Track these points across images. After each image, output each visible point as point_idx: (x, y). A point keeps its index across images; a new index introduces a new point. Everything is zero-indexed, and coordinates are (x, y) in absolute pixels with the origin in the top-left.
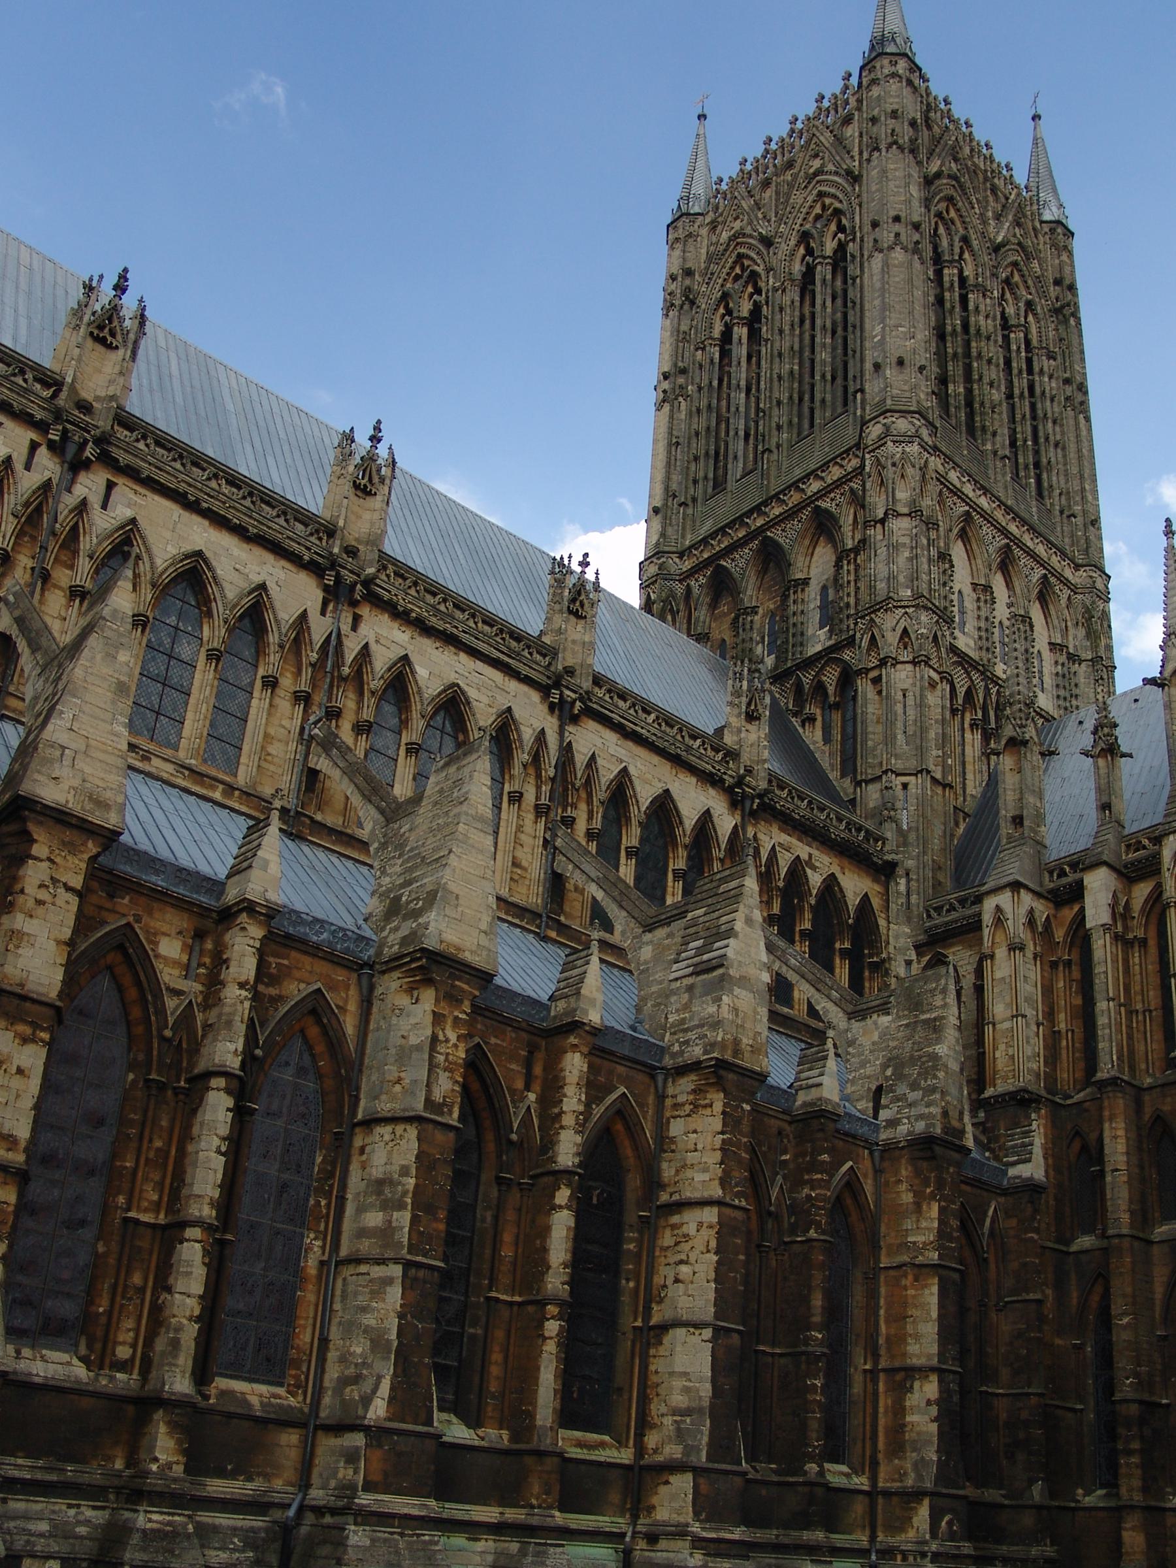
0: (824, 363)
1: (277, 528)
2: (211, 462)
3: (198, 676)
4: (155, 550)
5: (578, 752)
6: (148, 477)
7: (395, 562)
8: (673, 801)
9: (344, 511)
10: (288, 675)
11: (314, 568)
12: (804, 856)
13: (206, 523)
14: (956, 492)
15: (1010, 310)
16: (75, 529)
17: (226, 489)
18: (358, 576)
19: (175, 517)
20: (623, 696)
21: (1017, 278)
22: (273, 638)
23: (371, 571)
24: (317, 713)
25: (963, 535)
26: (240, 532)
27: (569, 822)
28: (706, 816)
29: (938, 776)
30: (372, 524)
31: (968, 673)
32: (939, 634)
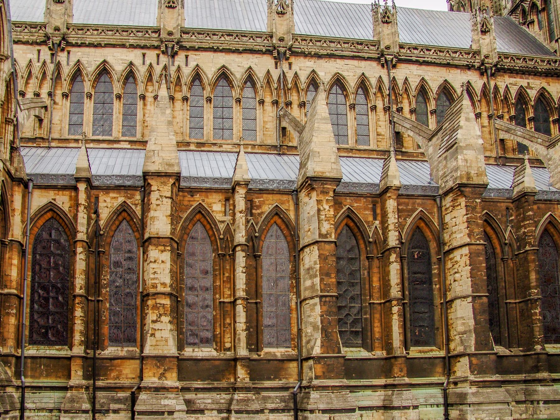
1: (250, 44)
2: (219, 31)
3: (234, 110)
4: (207, 72)
6: (199, 48)
7: (301, 35)
9: (274, 25)
10: (268, 96)
11: (268, 52)
13: (224, 54)
16: (178, 77)
17: (228, 38)
18: (286, 47)
19: (212, 57)
22: (258, 85)
23: (290, 43)
24: (282, 105)
26: (237, 51)
30: (287, 25)
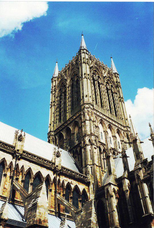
0: (75, 98)
5: (20, 165)
8: (41, 173)
12: (70, 182)
14: (99, 116)
15: (108, 87)
20: (30, 154)
21: (109, 82)
25: (101, 123)
27: (17, 179)
28: (48, 175)
29: (98, 165)
31: (103, 146)
32: (96, 139)
